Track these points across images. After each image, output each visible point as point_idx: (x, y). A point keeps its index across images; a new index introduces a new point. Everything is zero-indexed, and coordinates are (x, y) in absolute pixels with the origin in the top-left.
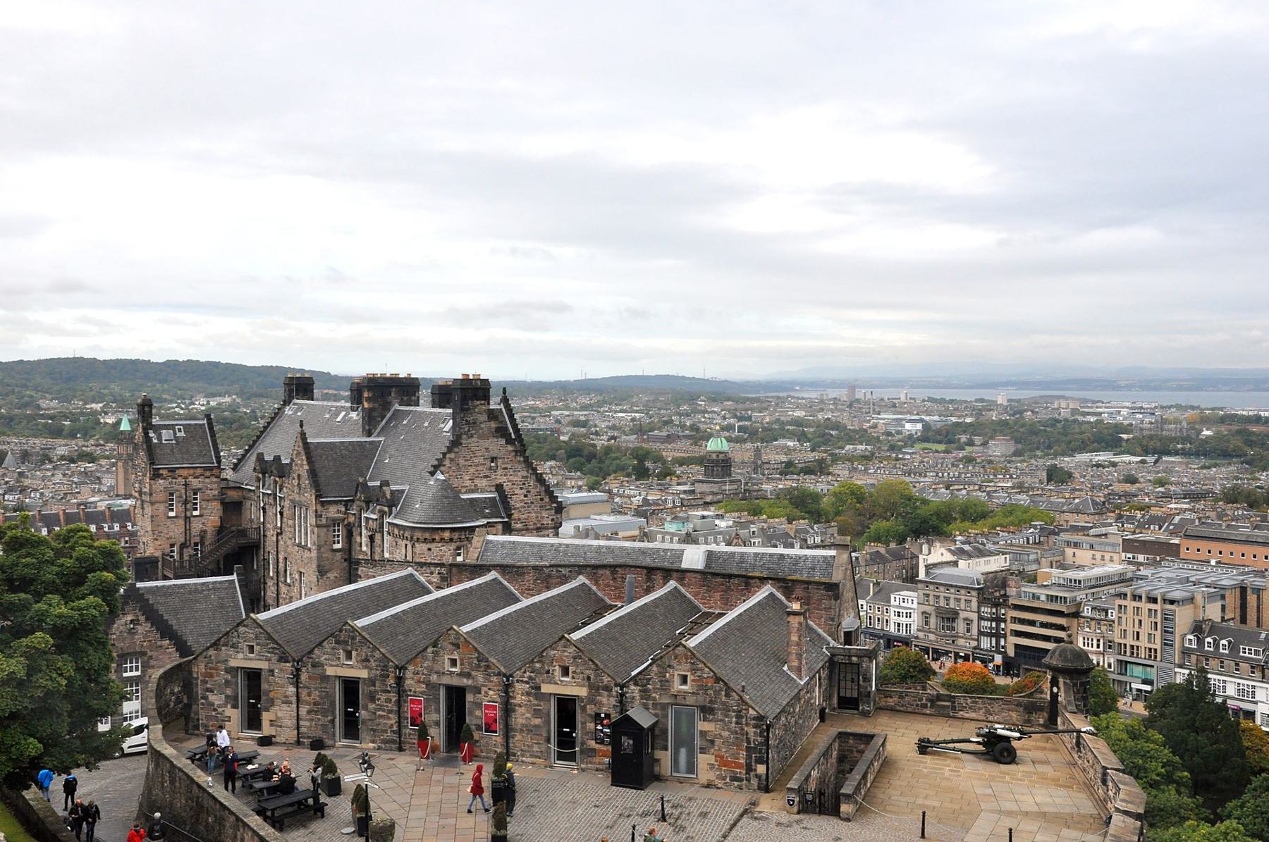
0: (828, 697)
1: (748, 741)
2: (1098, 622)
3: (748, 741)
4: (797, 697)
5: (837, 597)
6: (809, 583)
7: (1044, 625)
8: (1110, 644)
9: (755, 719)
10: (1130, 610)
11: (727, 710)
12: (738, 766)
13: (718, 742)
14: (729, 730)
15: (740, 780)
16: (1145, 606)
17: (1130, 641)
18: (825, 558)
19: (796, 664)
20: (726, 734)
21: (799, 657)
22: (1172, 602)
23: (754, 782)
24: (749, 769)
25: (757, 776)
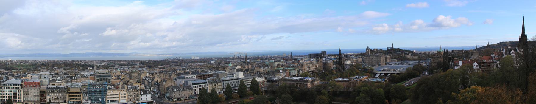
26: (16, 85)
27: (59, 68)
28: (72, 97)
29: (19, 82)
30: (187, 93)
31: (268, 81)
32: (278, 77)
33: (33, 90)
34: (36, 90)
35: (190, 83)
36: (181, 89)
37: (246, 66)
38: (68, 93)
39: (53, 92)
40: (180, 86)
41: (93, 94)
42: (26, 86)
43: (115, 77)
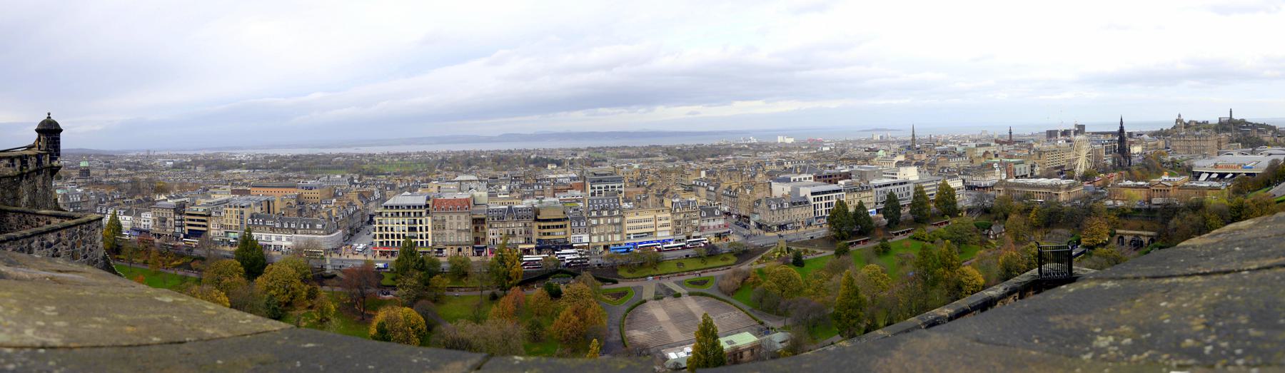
26: (415, 207)
27: (481, 167)
28: (546, 231)
29: (421, 200)
30: (800, 213)
31: (971, 188)
32: (989, 180)
33: (455, 217)
34: (463, 216)
35: (805, 192)
36: (786, 205)
37: (916, 156)
38: (536, 220)
39: (501, 219)
40: (784, 197)
41: (594, 222)
43: (631, 181)
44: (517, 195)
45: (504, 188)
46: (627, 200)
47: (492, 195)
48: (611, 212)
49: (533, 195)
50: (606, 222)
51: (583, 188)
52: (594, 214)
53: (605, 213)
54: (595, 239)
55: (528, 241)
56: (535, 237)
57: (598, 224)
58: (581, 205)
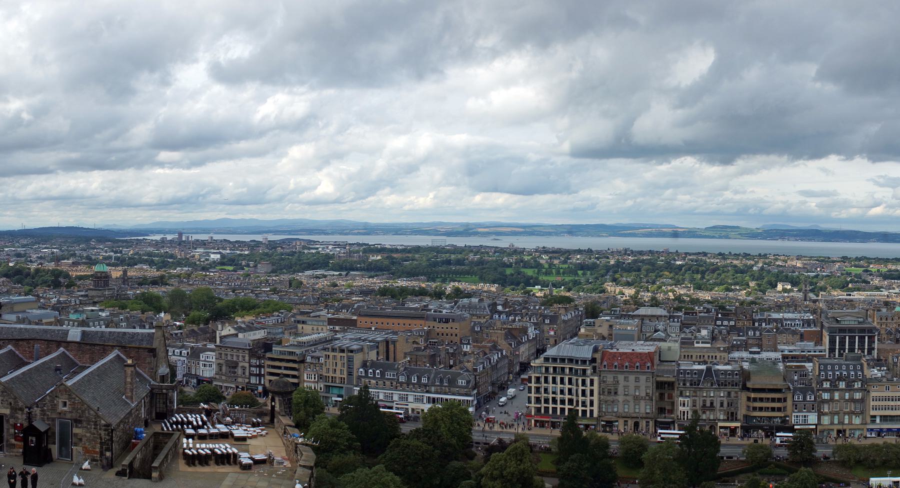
0: (149, 413)
1: (101, 439)
2: (315, 365)
3: (101, 439)
4: (130, 413)
5: (155, 356)
6: (139, 348)
7: (286, 368)
8: (321, 377)
9: (105, 426)
10: (331, 357)
11: (88, 421)
12: (96, 453)
13: (84, 439)
14: (90, 432)
15: (97, 461)
16: (339, 355)
17: (331, 374)
18: (149, 334)
19: (130, 394)
20: (88, 435)
21: (132, 390)
22: (352, 351)
23: (105, 462)
24: (102, 454)
25: (107, 458)
28: (758, 404)
38: (745, 388)
41: (826, 396)
42: (611, 365)
44: (721, 345)
45: (704, 332)
46: (878, 363)
47: (686, 343)
48: (850, 388)
49: (745, 346)
50: (842, 398)
51: (819, 341)
52: (826, 385)
53: (842, 385)
54: (826, 420)
55: (732, 417)
56: (742, 412)
57: (832, 399)
58: (809, 366)
